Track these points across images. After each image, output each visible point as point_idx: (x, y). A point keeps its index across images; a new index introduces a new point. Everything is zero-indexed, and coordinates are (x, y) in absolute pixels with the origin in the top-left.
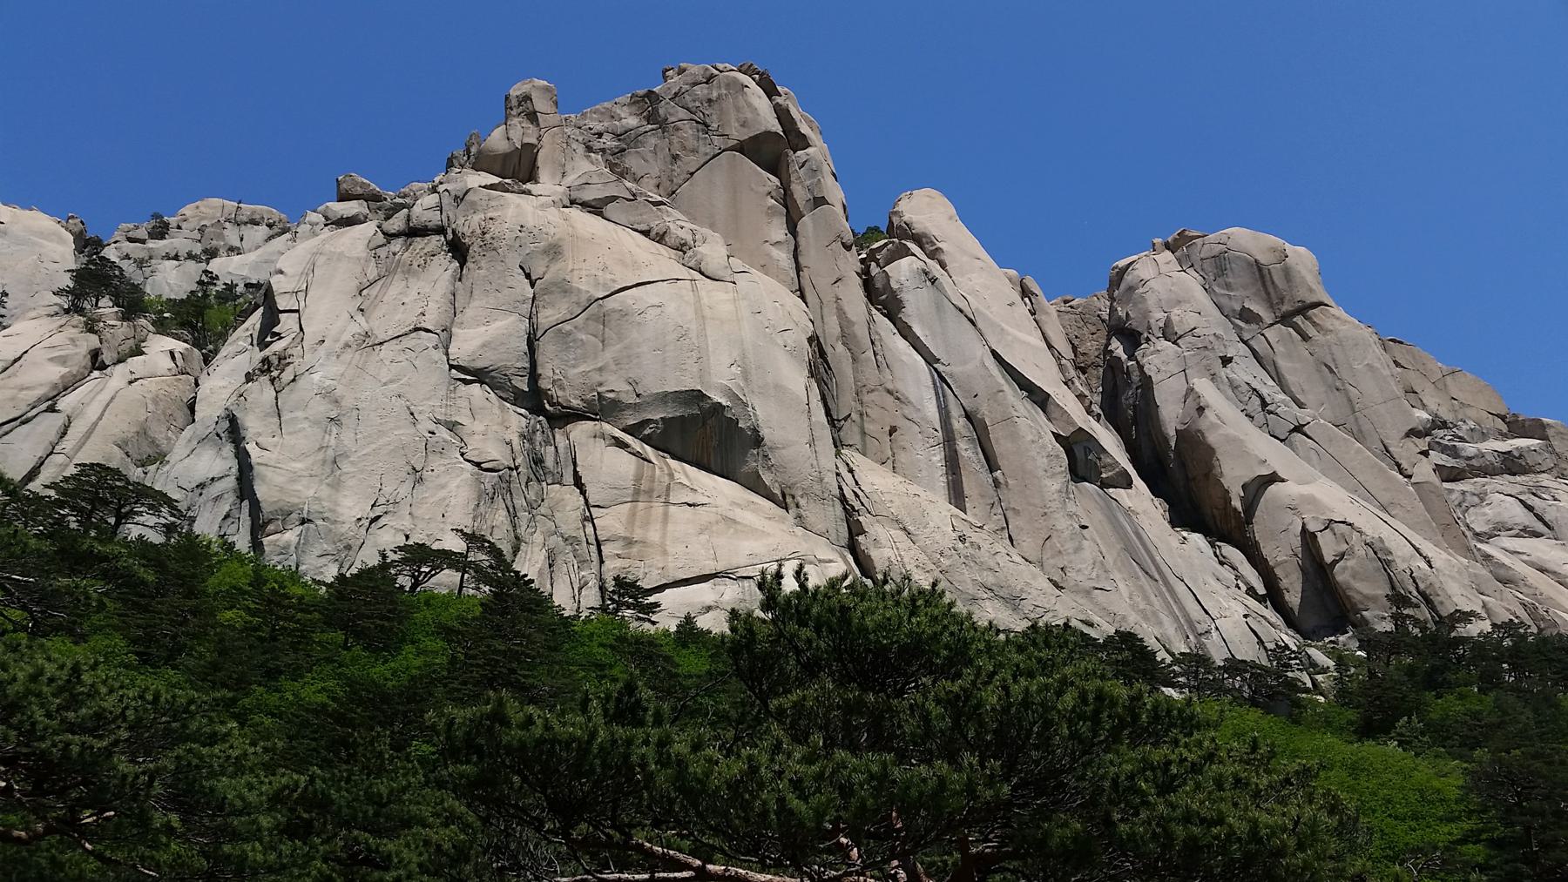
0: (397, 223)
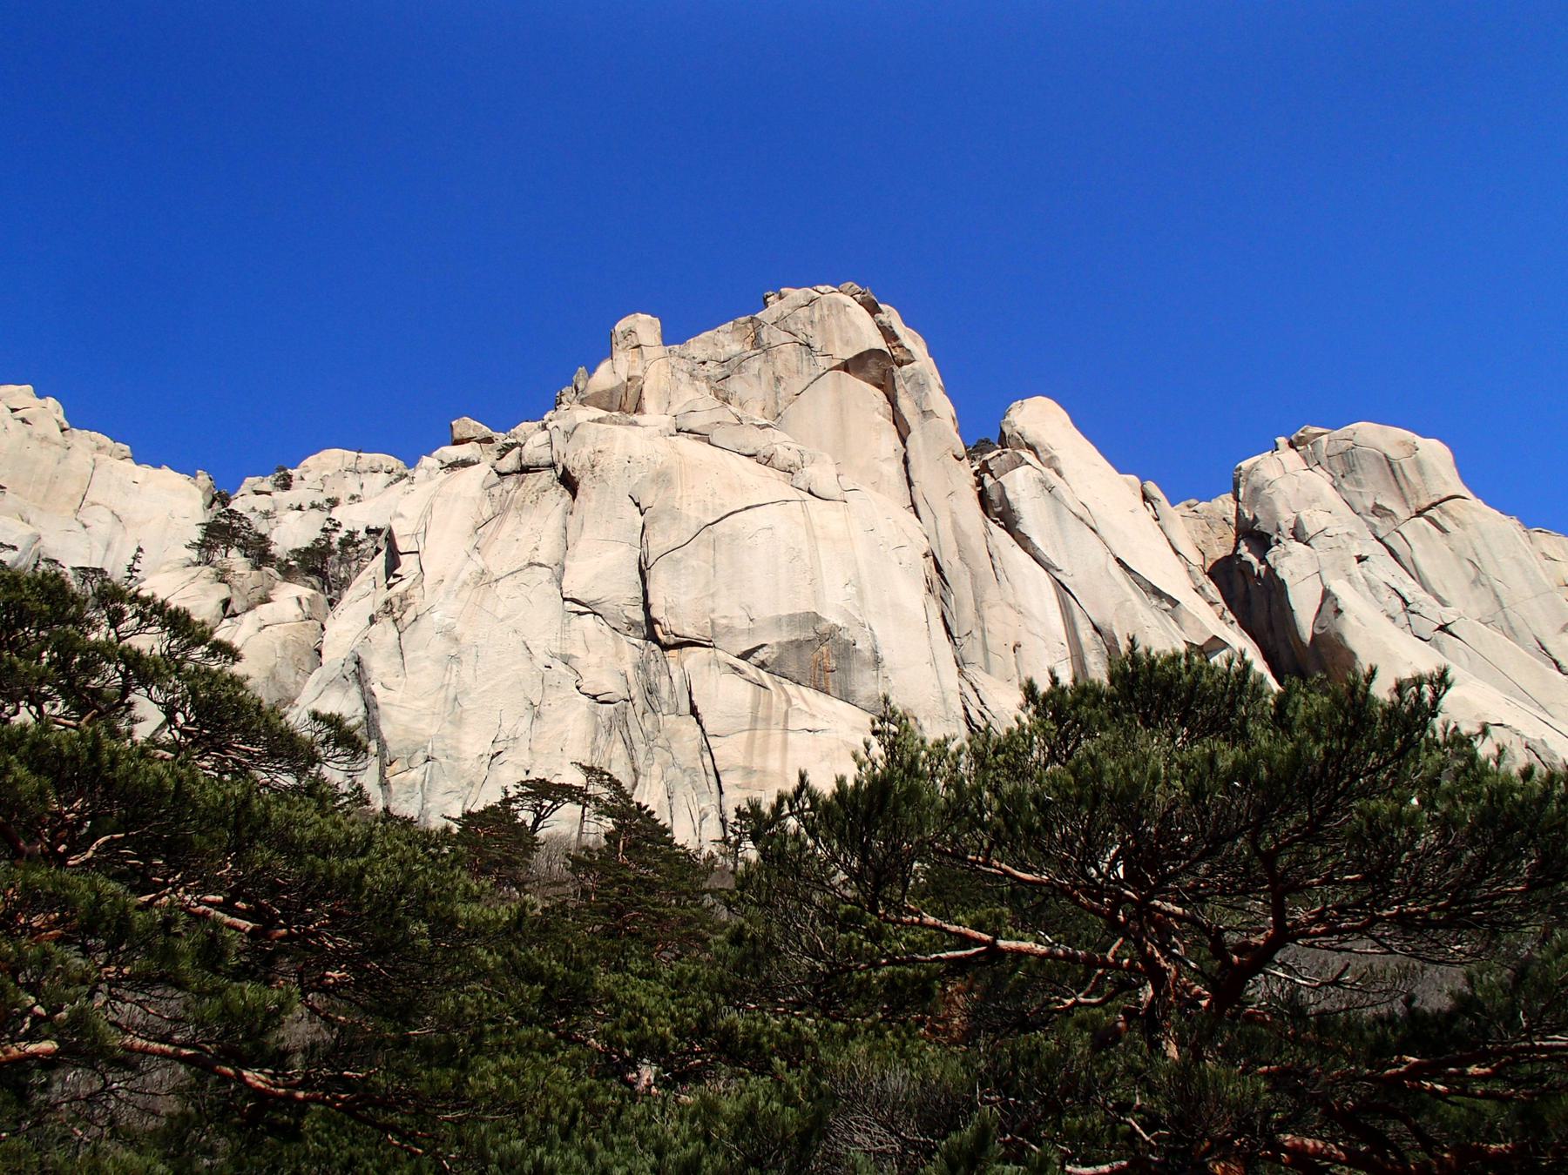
0: (509, 462)
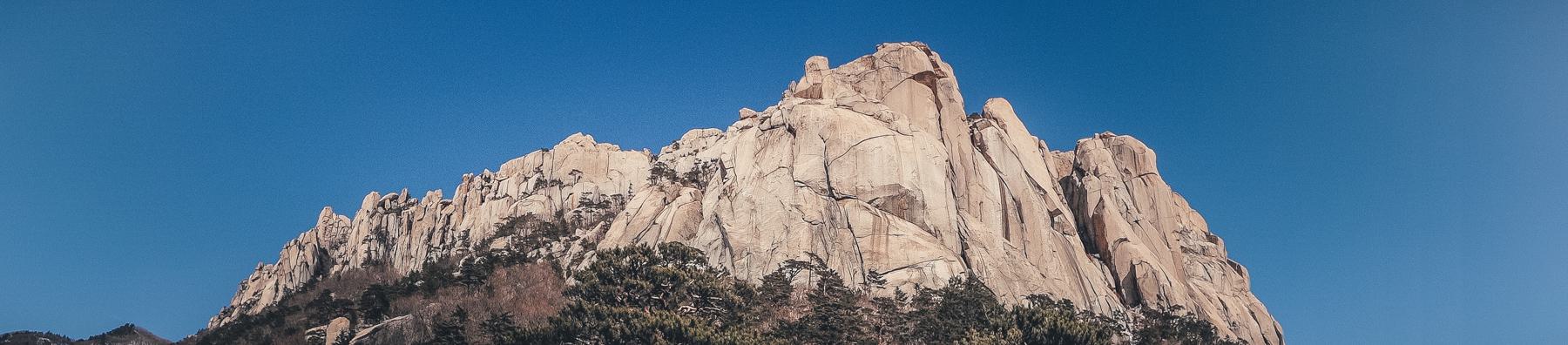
0: (766, 125)
